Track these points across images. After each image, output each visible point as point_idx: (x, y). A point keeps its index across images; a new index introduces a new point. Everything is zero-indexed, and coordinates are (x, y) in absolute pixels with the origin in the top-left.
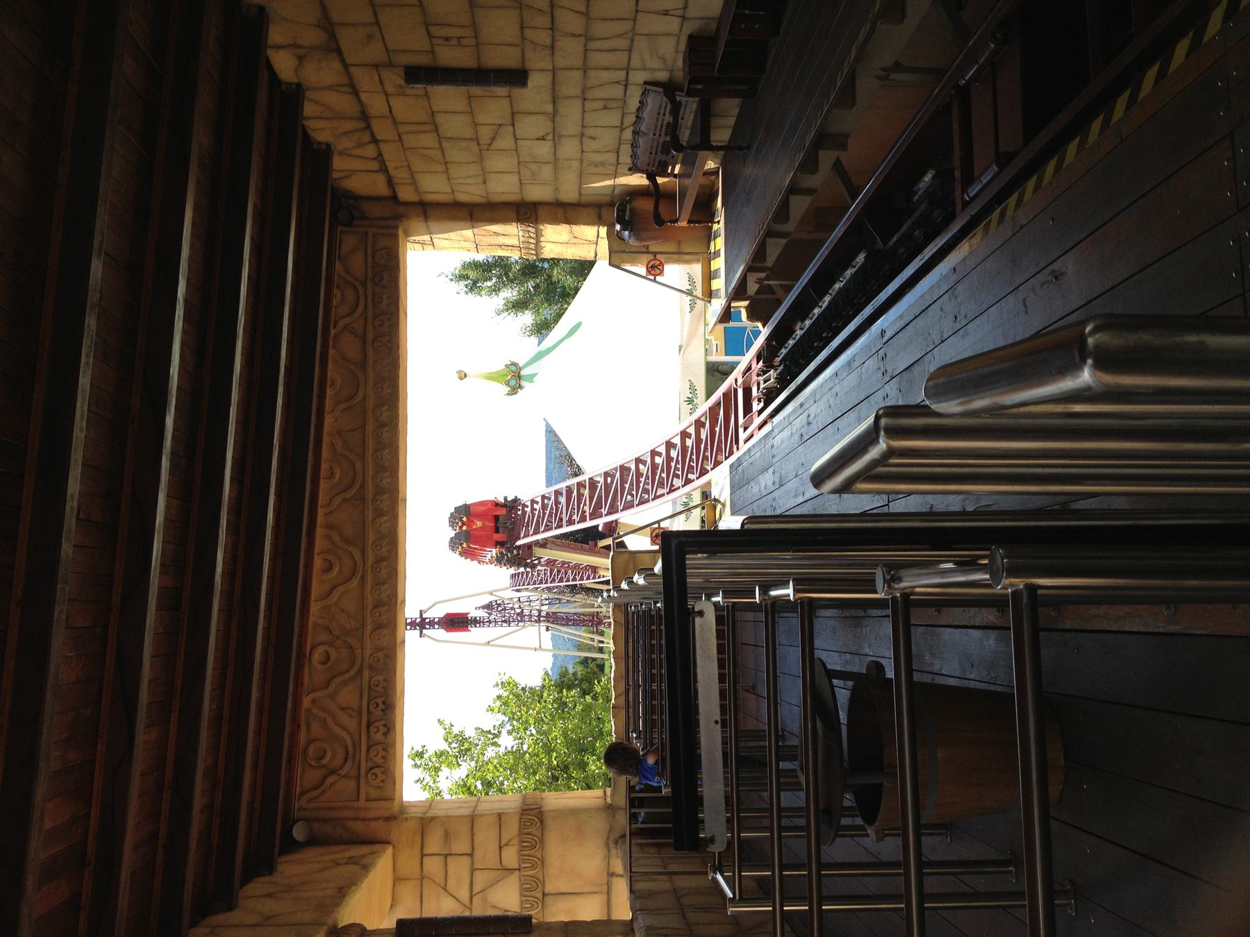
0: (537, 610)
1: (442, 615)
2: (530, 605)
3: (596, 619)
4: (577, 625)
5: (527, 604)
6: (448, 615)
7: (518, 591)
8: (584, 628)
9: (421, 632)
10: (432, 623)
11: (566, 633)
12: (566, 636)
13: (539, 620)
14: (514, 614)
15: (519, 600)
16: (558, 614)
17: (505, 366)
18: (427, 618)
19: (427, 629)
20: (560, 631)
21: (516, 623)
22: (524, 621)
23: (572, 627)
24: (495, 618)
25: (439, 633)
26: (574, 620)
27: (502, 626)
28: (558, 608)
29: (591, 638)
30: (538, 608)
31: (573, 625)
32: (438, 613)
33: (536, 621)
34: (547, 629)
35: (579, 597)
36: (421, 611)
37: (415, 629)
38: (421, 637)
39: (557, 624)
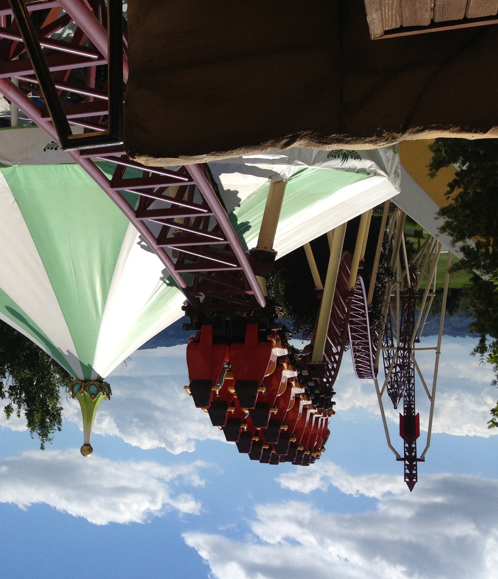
0: (398, 351)
1: (402, 440)
2: (392, 358)
3: (408, 295)
4: (413, 313)
5: (391, 361)
6: (402, 434)
7: (376, 371)
8: (417, 308)
9: (420, 460)
10: (410, 450)
11: (421, 323)
12: (425, 324)
13: (407, 349)
14: (401, 373)
15: (387, 368)
16: (402, 330)
17: (73, 398)
18: (405, 454)
19: (416, 454)
20: (420, 329)
21: (411, 370)
22: (409, 363)
23: (416, 318)
24: (406, 391)
25: (420, 443)
26: (408, 315)
27: (414, 384)
28: (396, 331)
29: (427, 300)
30: (395, 351)
31: (413, 317)
32: (399, 444)
33: (410, 352)
34: (418, 341)
35: (385, 311)
36: (398, 460)
37: (416, 465)
38: (424, 461)
39: (412, 332)
